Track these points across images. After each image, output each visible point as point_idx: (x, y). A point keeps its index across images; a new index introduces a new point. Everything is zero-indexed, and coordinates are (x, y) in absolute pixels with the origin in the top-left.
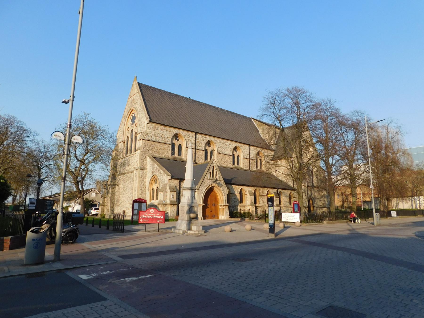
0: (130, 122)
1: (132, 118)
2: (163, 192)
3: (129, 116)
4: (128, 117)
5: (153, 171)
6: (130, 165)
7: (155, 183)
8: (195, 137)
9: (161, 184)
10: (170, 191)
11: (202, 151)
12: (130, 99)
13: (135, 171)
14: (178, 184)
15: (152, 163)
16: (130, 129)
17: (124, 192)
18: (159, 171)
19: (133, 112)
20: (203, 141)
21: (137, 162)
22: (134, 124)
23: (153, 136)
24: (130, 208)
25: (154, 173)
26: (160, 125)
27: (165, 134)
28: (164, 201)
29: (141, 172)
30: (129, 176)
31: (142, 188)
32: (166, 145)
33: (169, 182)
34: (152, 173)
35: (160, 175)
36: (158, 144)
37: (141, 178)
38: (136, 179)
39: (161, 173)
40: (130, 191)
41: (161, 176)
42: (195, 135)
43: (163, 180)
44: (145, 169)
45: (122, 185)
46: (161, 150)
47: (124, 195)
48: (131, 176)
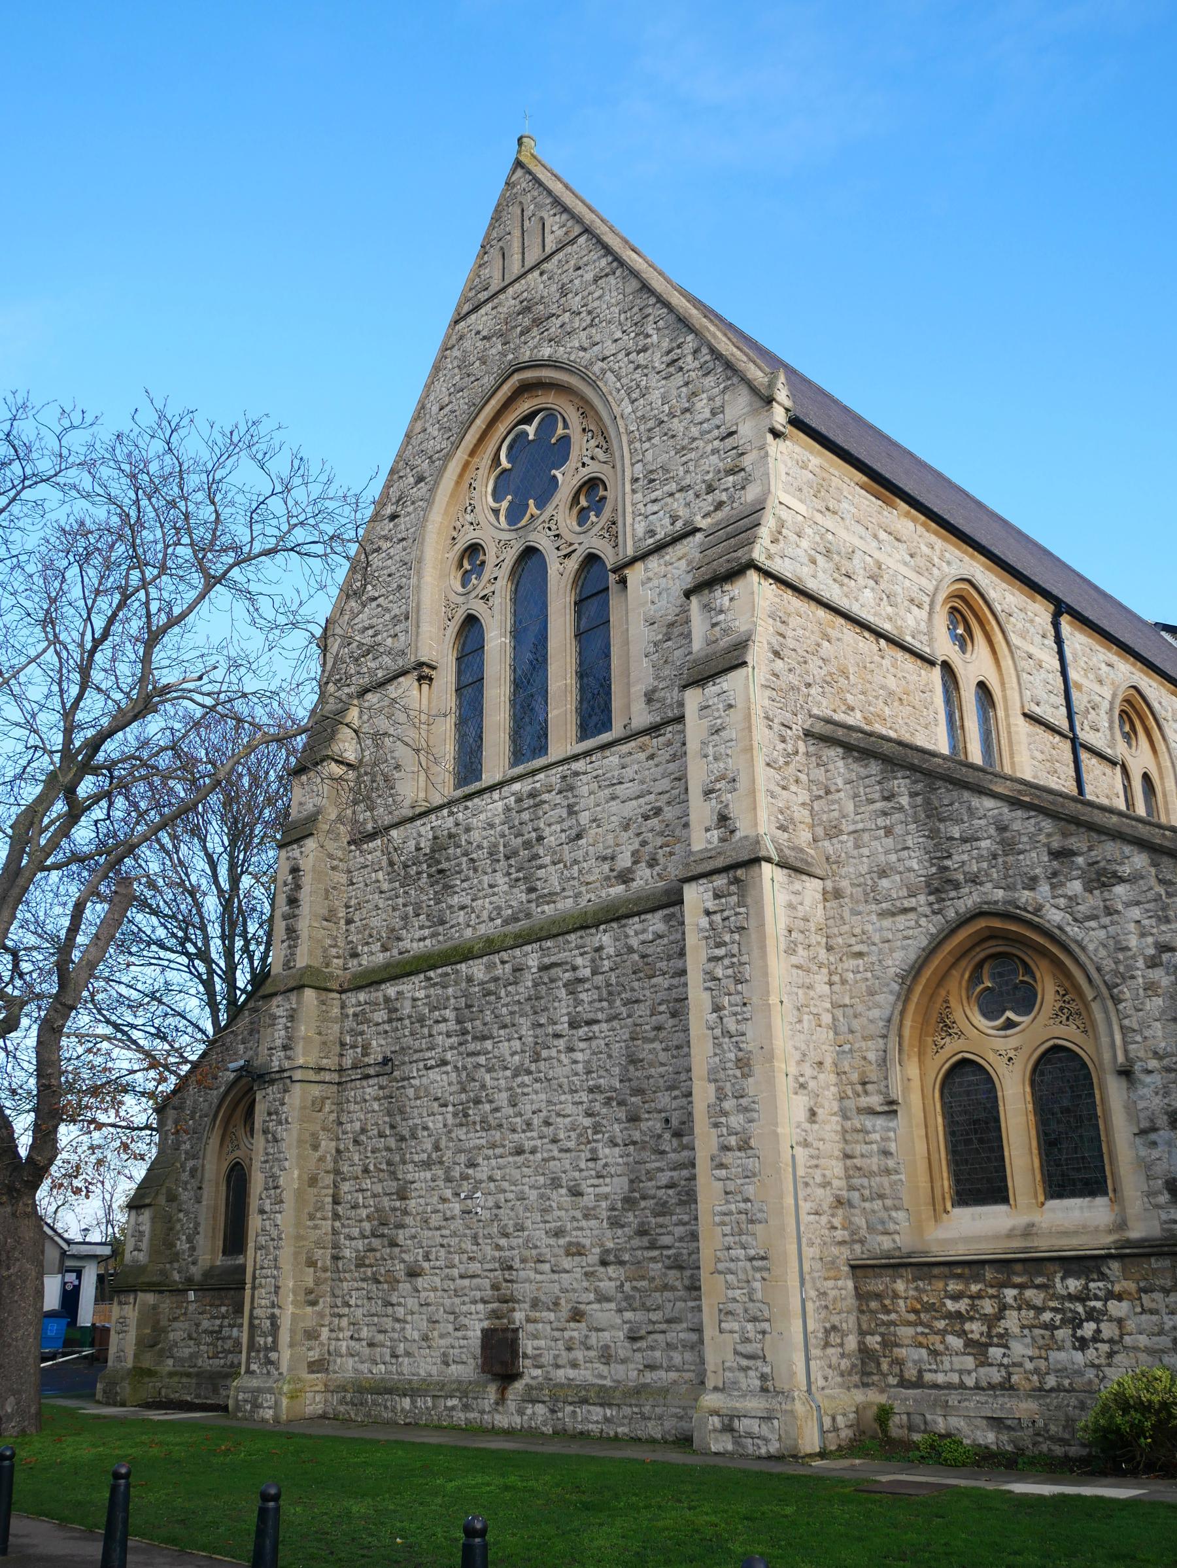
0: (490, 499)
1: (505, 463)
3: (472, 453)
4: (466, 465)
5: (946, 868)
6: (547, 860)
7: (976, 1008)
8: (1059, 641)
11: (1108, 770)
12: (473, 317)
13: (696, 896)
15: (904, 801)
16: (491, 558)
17: (476, 1139)
18: (1062, 855)
19: (525, 406)
20: (1096, 687)
21: (708, 793)
22: (541, 505)
23: (820, 559)
24: (602, 1298)
25: (968, 899)
29: (782, 898)
30: (544, 968)
31: (808, 1071)
34: (922, 899)
35: (1093, 901)
36: (868, 645)
37: (794, 960)
38: (719, 972)
39: (1125, 870)
40: (587, 1122)
42: (1056, 625)
44: (807, 863)
45: (444, 1063)
47: (472, 1165)
48: (579, 961)
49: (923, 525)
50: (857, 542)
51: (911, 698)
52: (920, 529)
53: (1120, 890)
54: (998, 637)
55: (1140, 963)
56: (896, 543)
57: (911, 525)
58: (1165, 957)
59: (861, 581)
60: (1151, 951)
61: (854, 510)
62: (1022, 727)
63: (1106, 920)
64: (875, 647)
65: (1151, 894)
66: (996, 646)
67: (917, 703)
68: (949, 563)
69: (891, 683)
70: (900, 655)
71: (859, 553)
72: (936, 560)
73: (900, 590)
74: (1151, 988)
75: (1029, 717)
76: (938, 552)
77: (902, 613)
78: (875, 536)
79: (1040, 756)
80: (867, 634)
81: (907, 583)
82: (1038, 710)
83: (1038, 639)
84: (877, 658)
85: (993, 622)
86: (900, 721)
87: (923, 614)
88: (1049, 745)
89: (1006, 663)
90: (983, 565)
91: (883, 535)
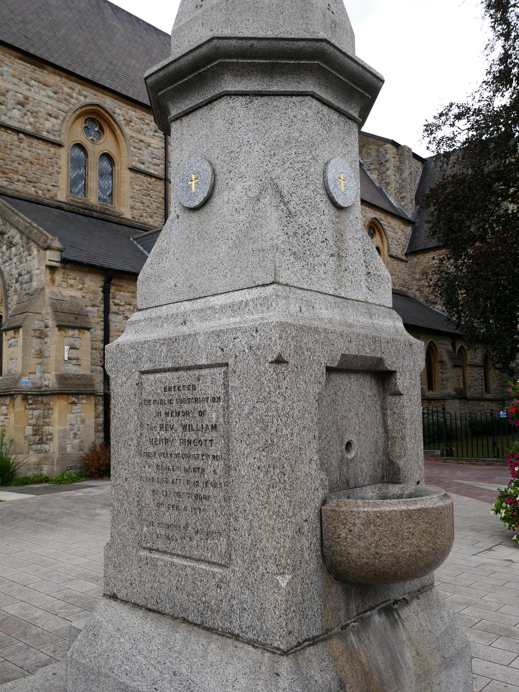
2: (21, 330)
9: (16, 297)
10: (55, 323)
14: (101, 294)
26: (15, 54)
27: (37, 97)
28: (24, 379)
32: (42, 145)
33: (53, 281)
39: (15, 241)
41: (15, 259)
43: (20, 275)
46: (19, 164)
49: (66, 78)
50: (10, 86)
51: (41, 162)
52: (64, 80)
53: (13, 249)
54: (118, 132)
55: (14, 281)
56: (45, 87)
57: (58, 78)
58: (20, 278)
59: (10, 106)
60: (17, 276)
61: (11, 71)
62: (128, 175)
63: (9, 262)
64: (15, 137)
65: (19, 252)
66: (117, 136)
67: (45, 164)
68: (85, 97)
69: (26, 154)
70: (35, 142)
71: (11, 93)
72: (74, 95)
73: (42, 110)
74: (15, 290)
75: (133, 170)
76: (77, 91)
77: (42, 121)
78: (27, 84)
79: (138, 187)
80: (10, 132)
81: (49, 107)
82: (142, 167)
83: (151, 133)
84: (17, 143)
85: (115, 125)
86: (30, 172)
87: (59, 121)
88: (146, 182)
89: (123, 144)
90: (112, 97)
91: (33, 83)
